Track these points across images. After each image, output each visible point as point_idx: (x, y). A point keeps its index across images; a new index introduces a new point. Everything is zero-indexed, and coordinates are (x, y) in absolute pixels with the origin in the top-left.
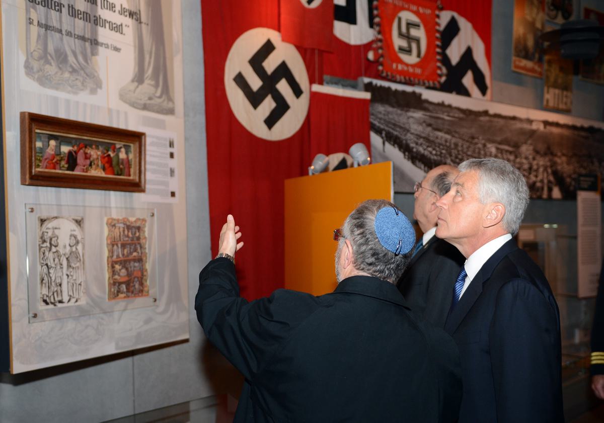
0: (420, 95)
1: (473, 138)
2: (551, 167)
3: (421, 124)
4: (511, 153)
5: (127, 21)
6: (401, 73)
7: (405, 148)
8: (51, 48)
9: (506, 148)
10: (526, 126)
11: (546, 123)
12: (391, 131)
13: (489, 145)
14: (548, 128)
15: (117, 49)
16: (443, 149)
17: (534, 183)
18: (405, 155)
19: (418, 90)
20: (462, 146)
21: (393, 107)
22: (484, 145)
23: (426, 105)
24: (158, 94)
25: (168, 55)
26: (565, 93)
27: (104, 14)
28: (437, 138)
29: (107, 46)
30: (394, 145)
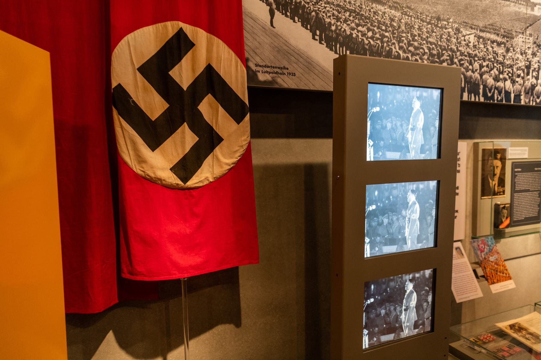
4: (499, 44)
9: (493, 37)
16: (386, 31)
17: (533, 87)
20: (420, 29)
22: (458, 30)
30: (293, 18)
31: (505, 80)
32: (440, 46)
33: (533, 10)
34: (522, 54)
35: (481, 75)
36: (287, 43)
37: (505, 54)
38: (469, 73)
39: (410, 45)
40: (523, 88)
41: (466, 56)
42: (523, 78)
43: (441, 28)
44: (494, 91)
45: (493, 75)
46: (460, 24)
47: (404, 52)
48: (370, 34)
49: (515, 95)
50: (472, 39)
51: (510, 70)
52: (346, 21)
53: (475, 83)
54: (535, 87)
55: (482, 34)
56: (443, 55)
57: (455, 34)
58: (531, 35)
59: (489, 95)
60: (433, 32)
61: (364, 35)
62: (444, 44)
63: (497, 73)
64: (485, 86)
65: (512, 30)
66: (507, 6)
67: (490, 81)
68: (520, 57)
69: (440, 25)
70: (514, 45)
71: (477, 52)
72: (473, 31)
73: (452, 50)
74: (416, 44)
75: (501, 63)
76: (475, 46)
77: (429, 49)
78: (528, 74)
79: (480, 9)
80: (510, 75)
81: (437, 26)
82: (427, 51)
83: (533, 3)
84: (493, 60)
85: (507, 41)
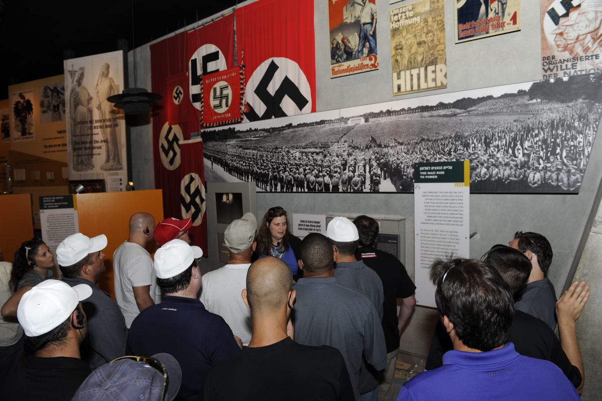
0: (234, 129)
1: (276, 148)
2: (377, 159)
3: (235, 148)
4: (317, 154)
5: (104, 144)
6: (218, 120)
7: (225, 165)
8: (79, 161)
9: (313, 150)
10: (337, 126)
11: (367, 117)
12: (216, 155)
13: (292, 152)
14: (371, 120)
15: (99, 154)
16: (251, 161)
17: (350, 178)
18: (225, 169)
19: (232, 126)
20: (267, 156)
21: (217, 141)
22: (288, 152)
23: (238, 134)
24: (116, 163)
25: (119, 149)
26: (431, 68)
27: (95, 145)
28: (246, 154)
29: (96, 154)
30: (218, 164)
31: (324, 176)
32: (278, 163)
33: (346, 123)
34: (338, 156)
35: (305, 176)
36: (217, 174)
37: (323, 159)
38: (297, 175)
39: (262, 165)
40: (341, 180)
41: (294, 165)
42: (339, 173)
43: (278, 153)
44: (315, 185)
45: (314, 174)
46: (289, 148)
47: (260, 169)
48: (244, 164)
49: (333, 186)
50: (298, 155)
51: (328, 169)
52: (235, 161)
53: (301, 181)
54: (352, 178)
55: (304, 150)
56: (280, 167)
57: (286, 154)
58: (345, 141)
59: (312, 187)
60: (274, 156)
61: (242, 165)
62: (280, 161)
63: (317, 172)
64: (308, 182)
65: (328, 142)
66: (323, 127)
67: (312, 178)
68: (337, 159)
69: (277, 152)
70: (330, 151)
71: (301, 161)
72: (298, 150)
73: (285, 164)
74: (265, 164)
75: (320, 165)
76: (300, 159)
77: (272, 165)
78: (345, 169)
79: (302, 135)
80: (328, 172)
81: (275, 152)
82: (271, 167)
83: (346, 118)
84: (313, 164)
85: (324, 150)
